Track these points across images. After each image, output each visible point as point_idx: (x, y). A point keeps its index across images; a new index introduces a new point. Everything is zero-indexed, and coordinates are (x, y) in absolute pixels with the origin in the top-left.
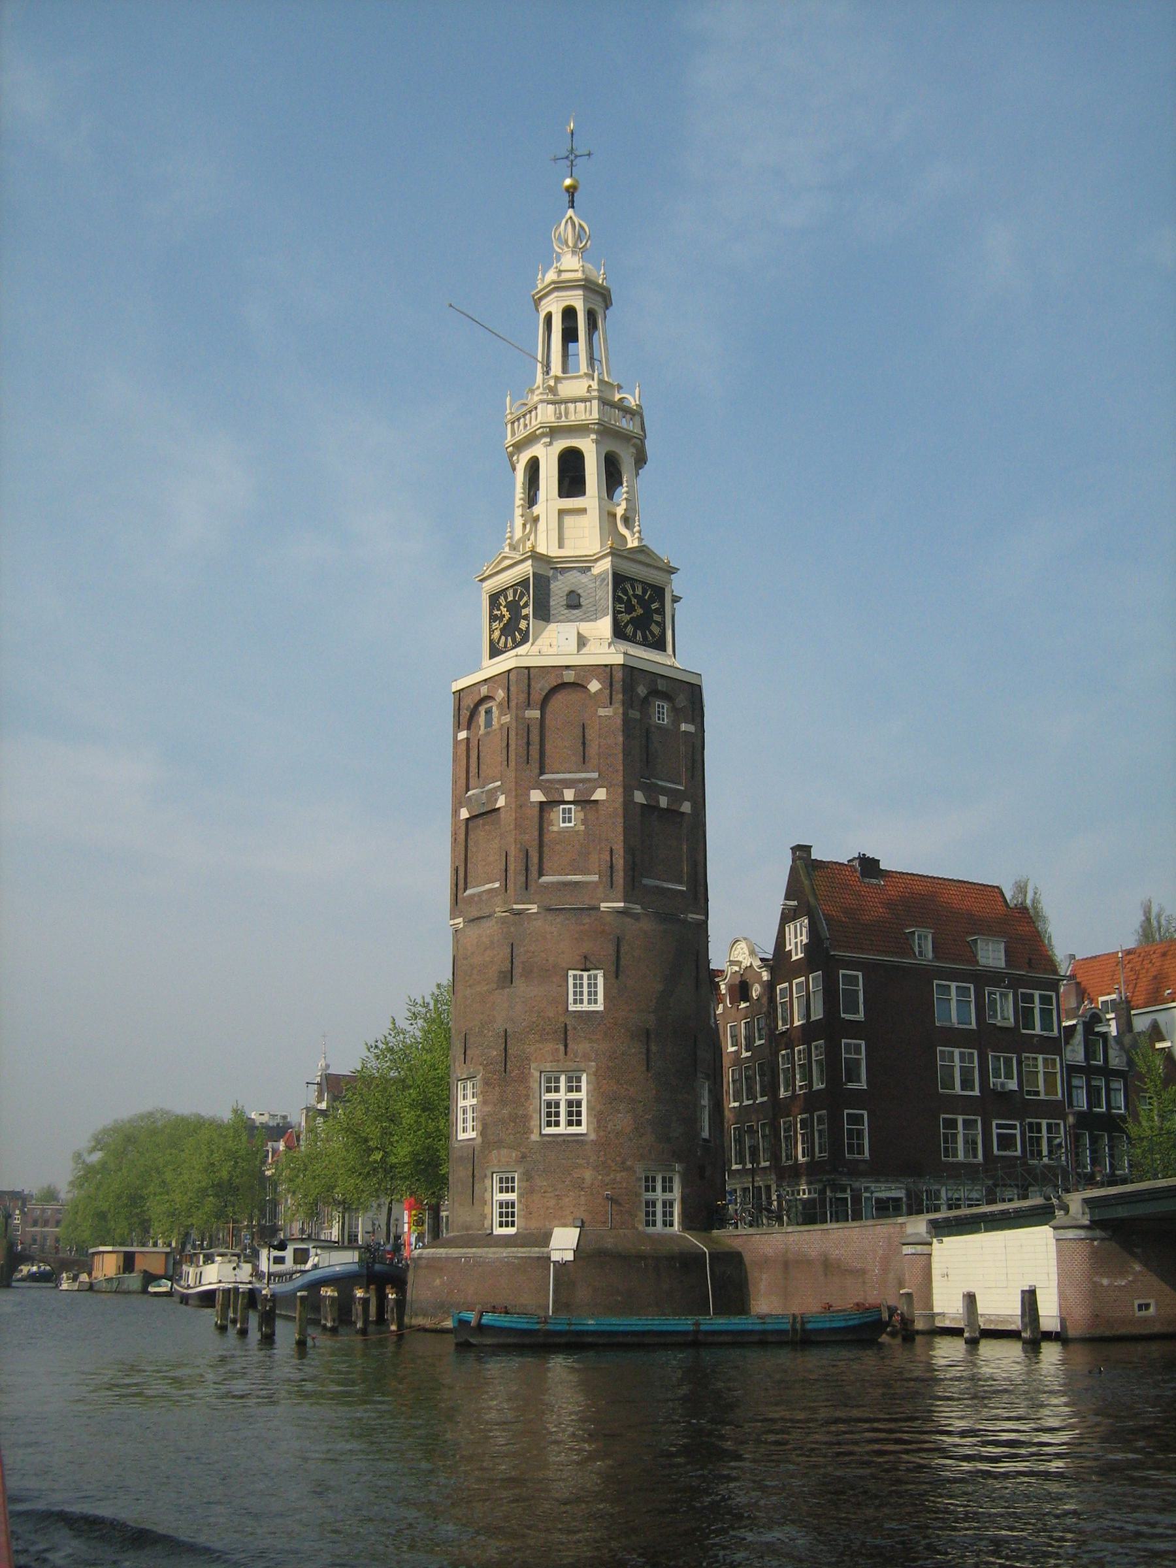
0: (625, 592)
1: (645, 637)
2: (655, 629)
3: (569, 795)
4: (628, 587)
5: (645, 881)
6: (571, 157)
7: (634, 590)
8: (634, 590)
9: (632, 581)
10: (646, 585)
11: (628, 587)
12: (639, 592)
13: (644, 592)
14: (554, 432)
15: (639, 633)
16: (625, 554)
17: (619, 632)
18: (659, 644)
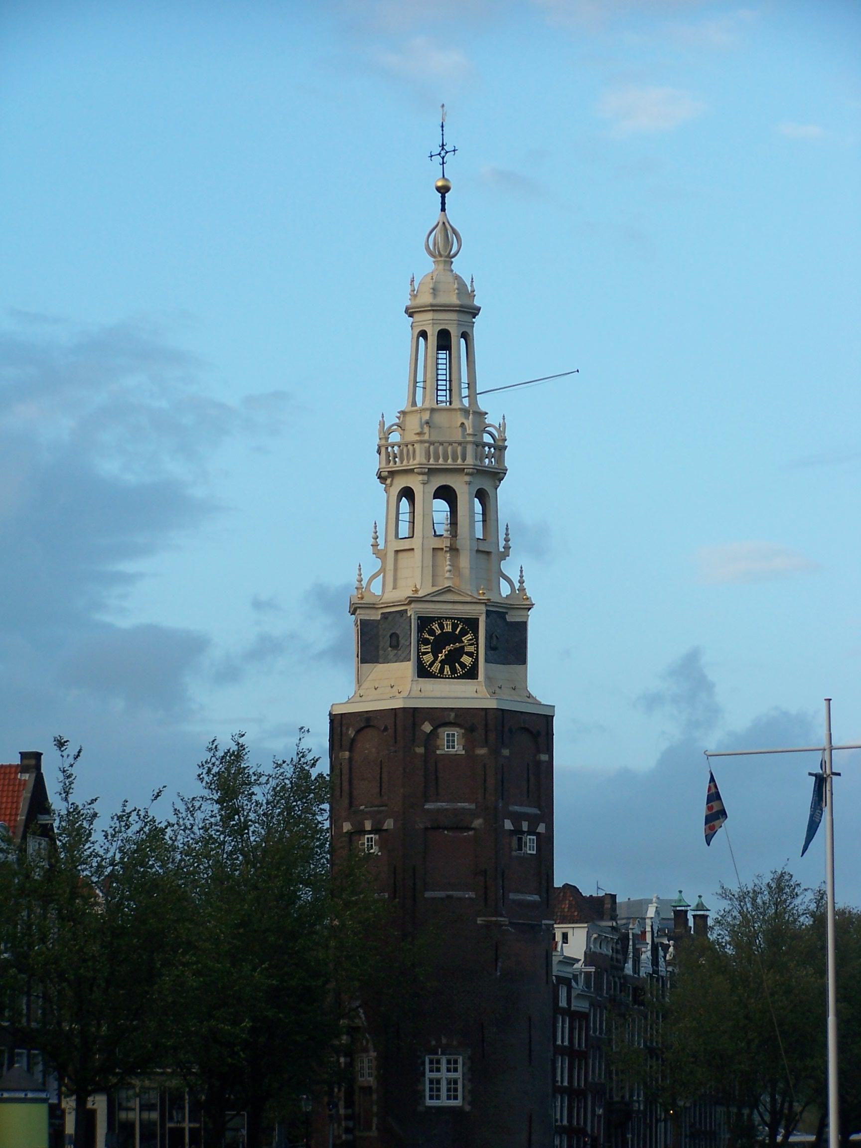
0: (432, 632)
1: (453, 670)
2: (467, 660)
3: (368, 826)
4: (435, 626)
5: (428, 894)
6: (443, 153)
7: (441, 627)
8: (441, 627)
9: (440, 620)
10: (456, 620)
11: (435, 626)
12: (449, 629)
13: (455, 626)
14: (392, 474)
15: (447, 668)
16: (428, 598)
17: (423, 672)
18: (471, 674)
